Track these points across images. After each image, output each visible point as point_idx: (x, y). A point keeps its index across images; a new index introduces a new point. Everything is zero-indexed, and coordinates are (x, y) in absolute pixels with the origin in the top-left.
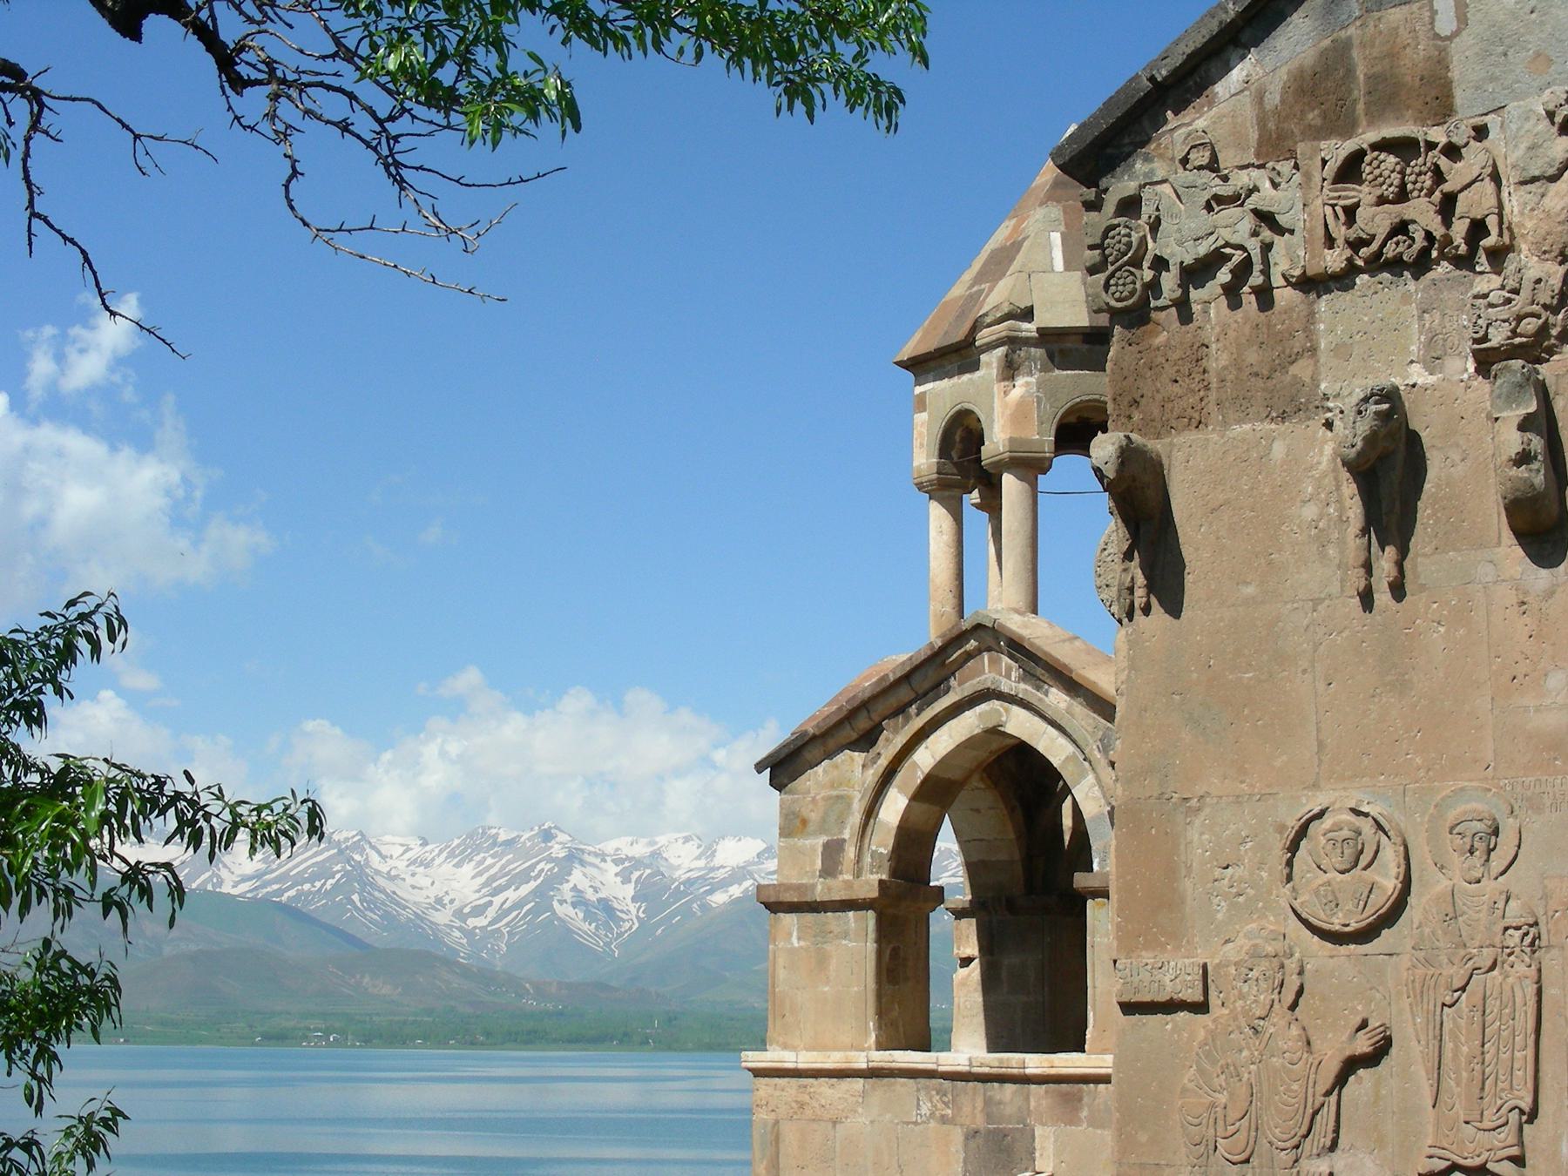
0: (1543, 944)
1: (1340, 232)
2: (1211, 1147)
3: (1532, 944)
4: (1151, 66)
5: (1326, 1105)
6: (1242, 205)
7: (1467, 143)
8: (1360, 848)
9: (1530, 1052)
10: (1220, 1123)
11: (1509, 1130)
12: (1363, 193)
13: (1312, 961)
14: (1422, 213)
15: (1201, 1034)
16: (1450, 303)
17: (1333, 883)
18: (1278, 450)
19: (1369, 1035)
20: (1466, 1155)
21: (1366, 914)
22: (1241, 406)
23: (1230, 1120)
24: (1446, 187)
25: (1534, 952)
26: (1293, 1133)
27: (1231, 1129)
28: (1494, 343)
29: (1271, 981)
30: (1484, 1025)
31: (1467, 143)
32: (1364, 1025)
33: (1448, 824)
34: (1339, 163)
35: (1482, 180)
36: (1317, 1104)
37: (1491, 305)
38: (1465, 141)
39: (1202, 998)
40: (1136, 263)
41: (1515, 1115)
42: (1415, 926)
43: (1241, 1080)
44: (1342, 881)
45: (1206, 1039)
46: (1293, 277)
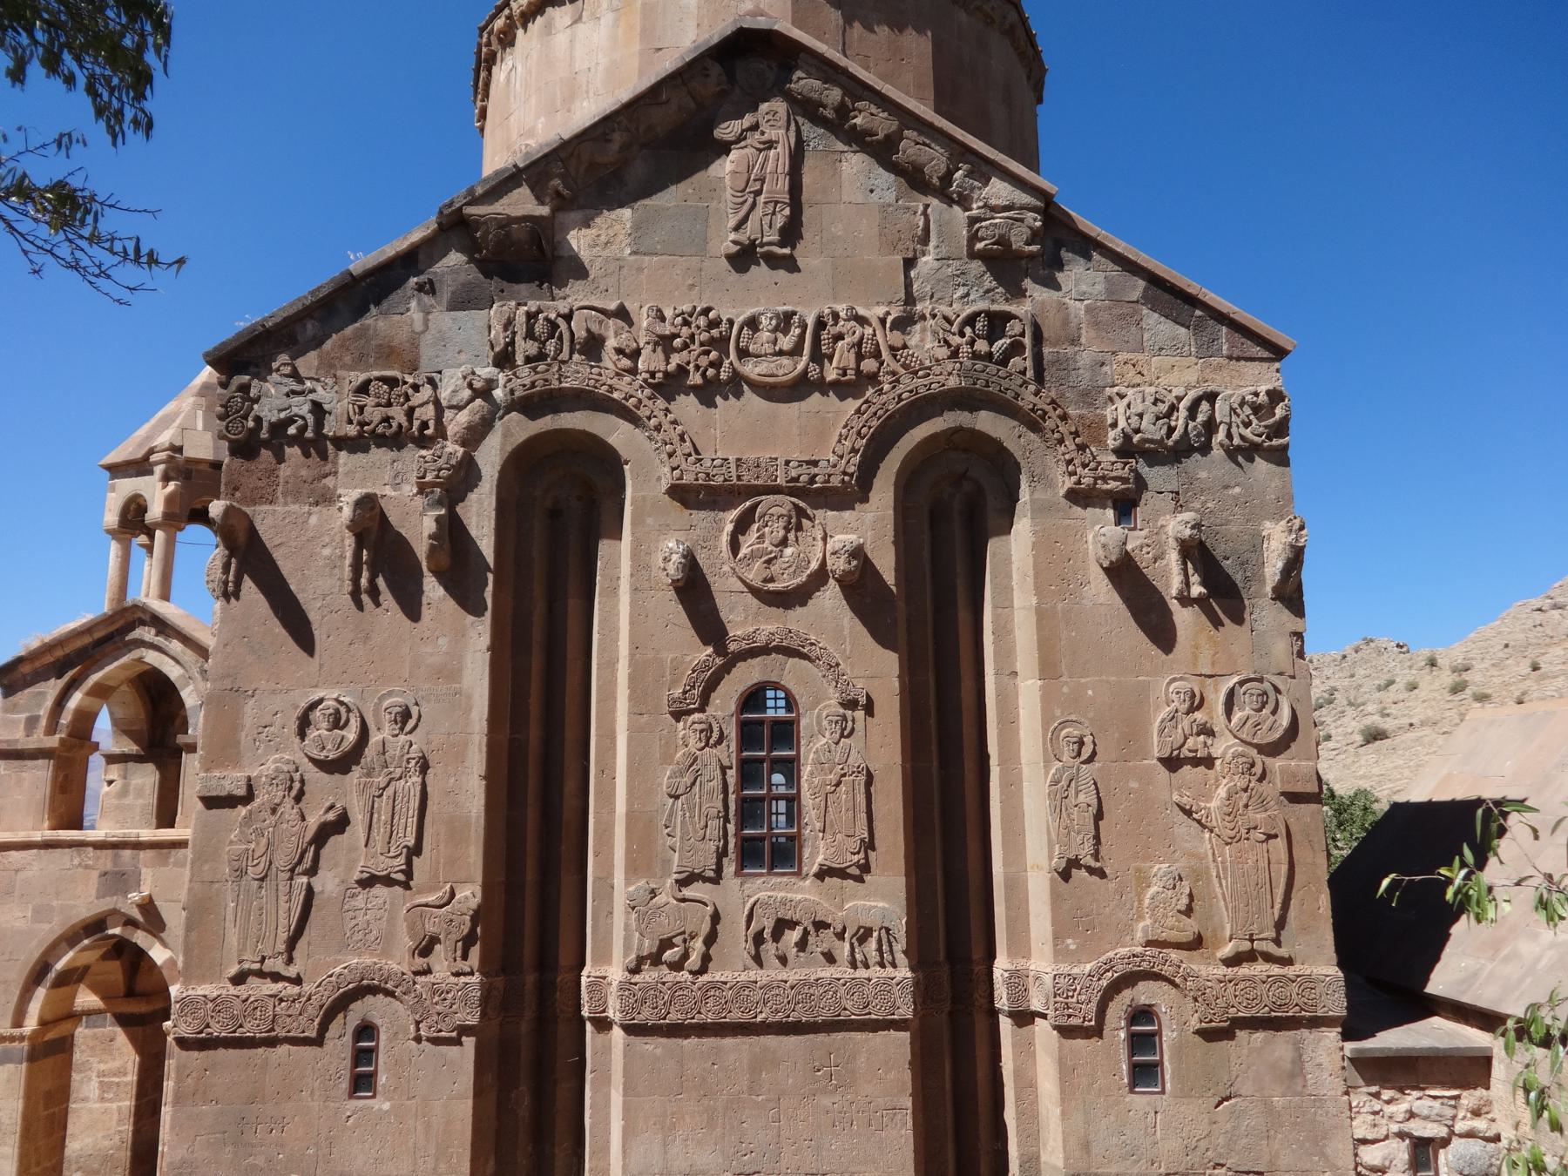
1: (356, 418)
4: (265, 319)
10: (250, 858)
12: (369, 401)
14: (398, 414)
18: (313, 520)
22: (296, 496)
24: (410, 403)
27: (256, 862)
28: (427, 479)
32: (332, 807)
37: (426, 462)
40: (245, 417)
41: (405, 850)
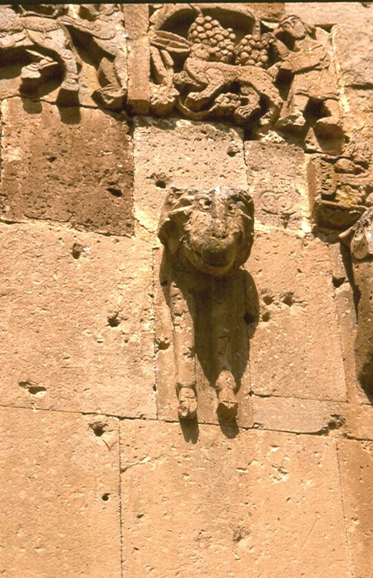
6: (55, 18)
7: (303, 38)
14: (261, 80)
16: (281, 167)
31: (303, 38)
34: (168, 14)
35: (320, 70)
38: (302, 34)
46: (109, 98)
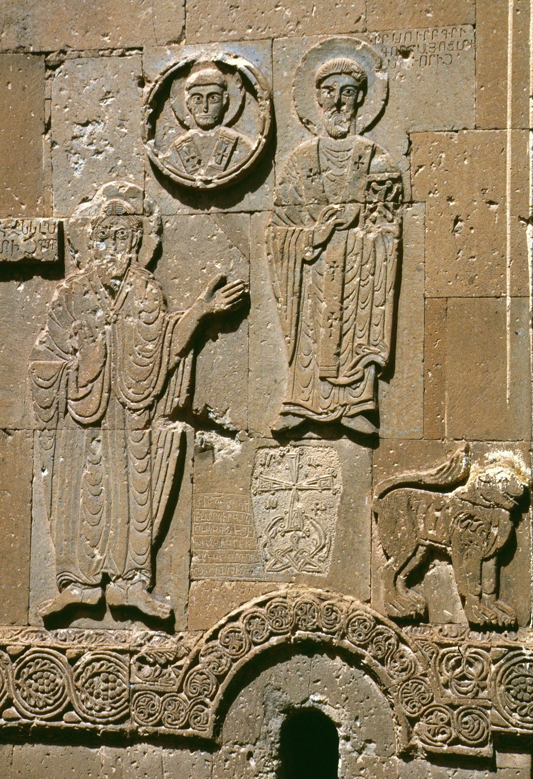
0: (407, 199)
2: (62, 409)
3: (395, 199)
5: (181, 365)
8: (225, 102)
9: (388, 308)
10: (72, 385)
11: (365, 385)
13: (172, 219)
15: (56, 294)
17: (196, 139)
19: (227, 293)
20: (321, 410)
21: (228, 171)
23: (82, 382)
25: (396, 207)
26: (146, 393)
27: (83, 392)
29: (128, 240)
30: (344, 280)
32: (222, 282)
33: (315, 78)
36: (172, 365)
39: (57, 258)
41: (372, 370)
42: (277, 182)
43: (94, 341)
44: (205, 137)
45: (60, 299)
